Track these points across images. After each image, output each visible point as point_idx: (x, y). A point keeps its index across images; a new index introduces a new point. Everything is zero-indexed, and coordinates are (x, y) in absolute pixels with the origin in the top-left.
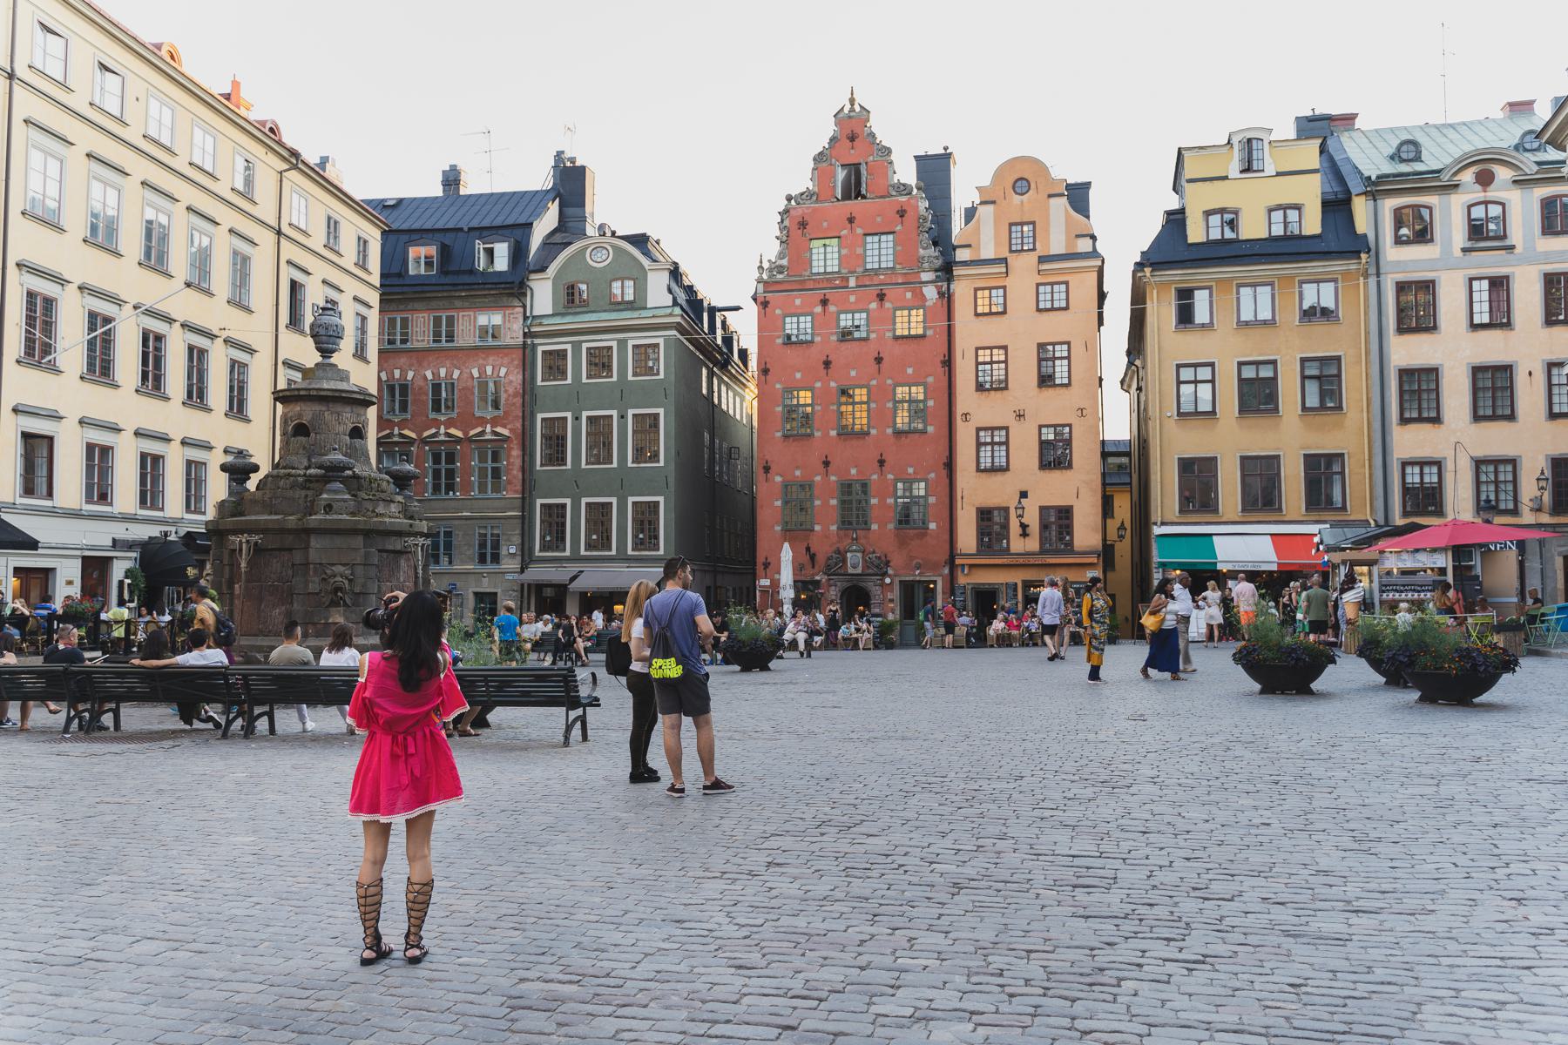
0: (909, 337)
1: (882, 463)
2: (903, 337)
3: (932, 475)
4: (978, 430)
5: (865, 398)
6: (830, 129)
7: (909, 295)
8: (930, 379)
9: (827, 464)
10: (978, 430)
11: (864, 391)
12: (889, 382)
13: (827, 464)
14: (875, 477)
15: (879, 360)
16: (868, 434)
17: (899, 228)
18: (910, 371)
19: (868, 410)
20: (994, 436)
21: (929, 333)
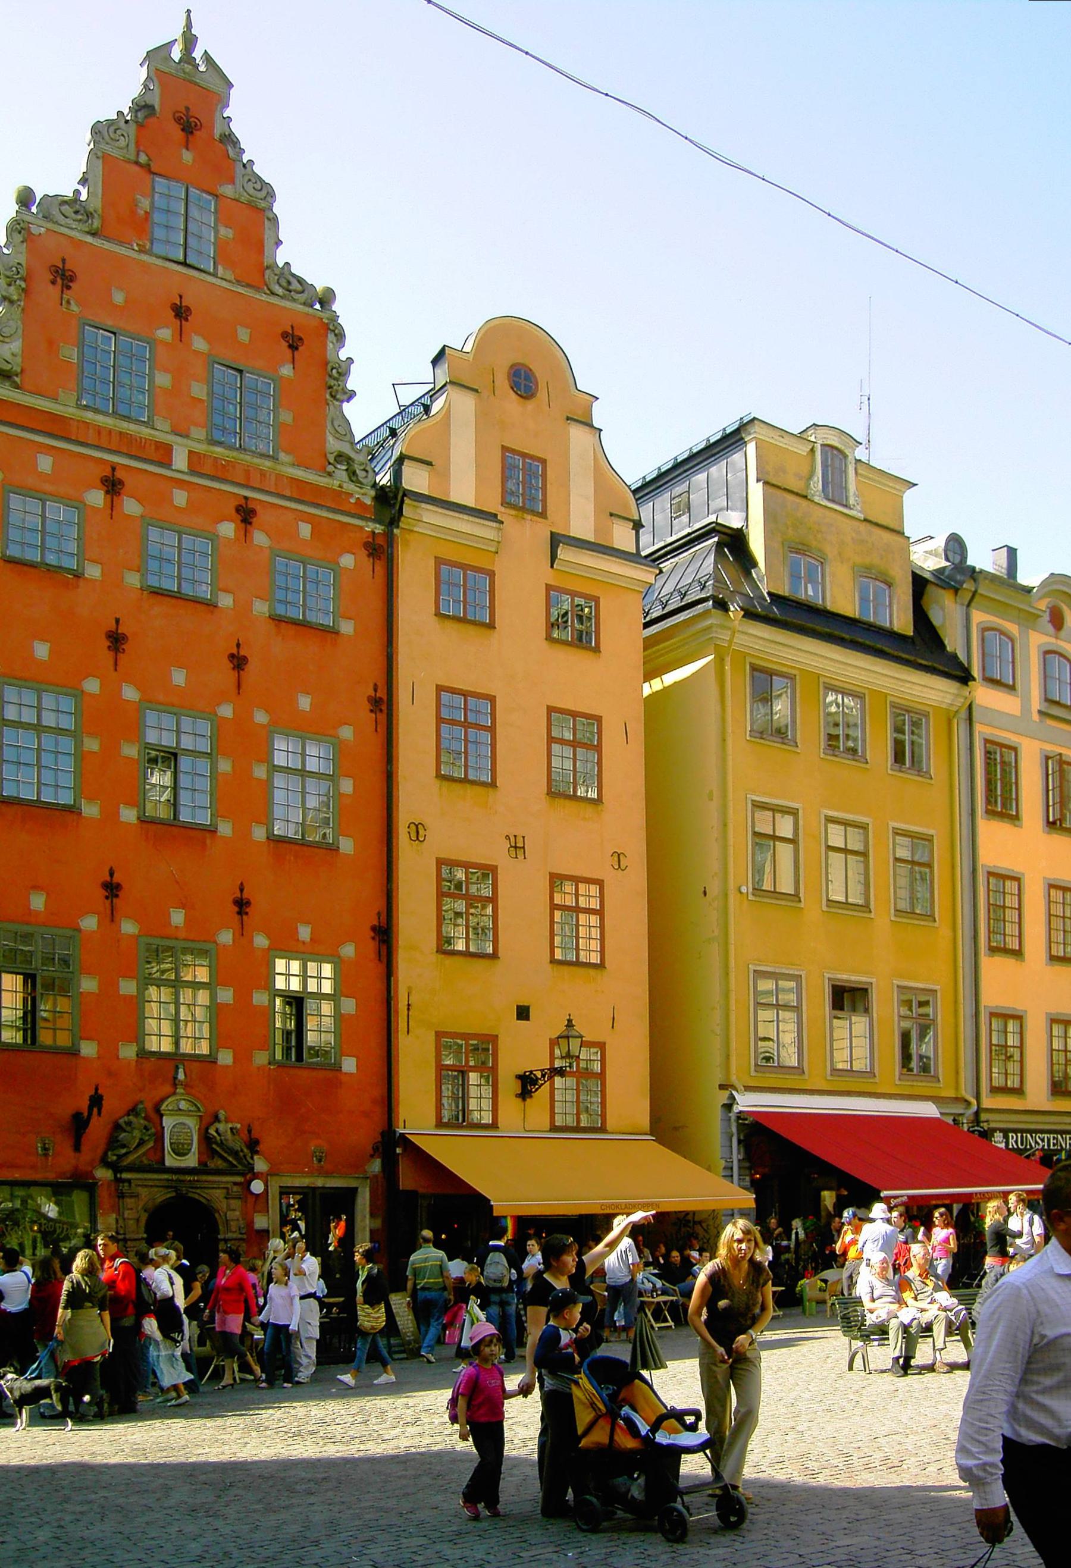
0: (303, 625)
1: (242, 905)
2: (295, 623)
3: (348, 950)
4: (440, 862)
5: (204, 746)
6: (120, 89)
7: (305, 530)
8: (347, 733)
9: (112, 889)
10: (440, 862)
11: (205, 727)
12: (261, 717)
13: (112, 889)
14: (226, 937)
15: (238, 662)
16: (212, 831)
17: (286, 371)
18: (305, 703)
19: (214, 774)
20: (467, 887)
21: (347, 628)
